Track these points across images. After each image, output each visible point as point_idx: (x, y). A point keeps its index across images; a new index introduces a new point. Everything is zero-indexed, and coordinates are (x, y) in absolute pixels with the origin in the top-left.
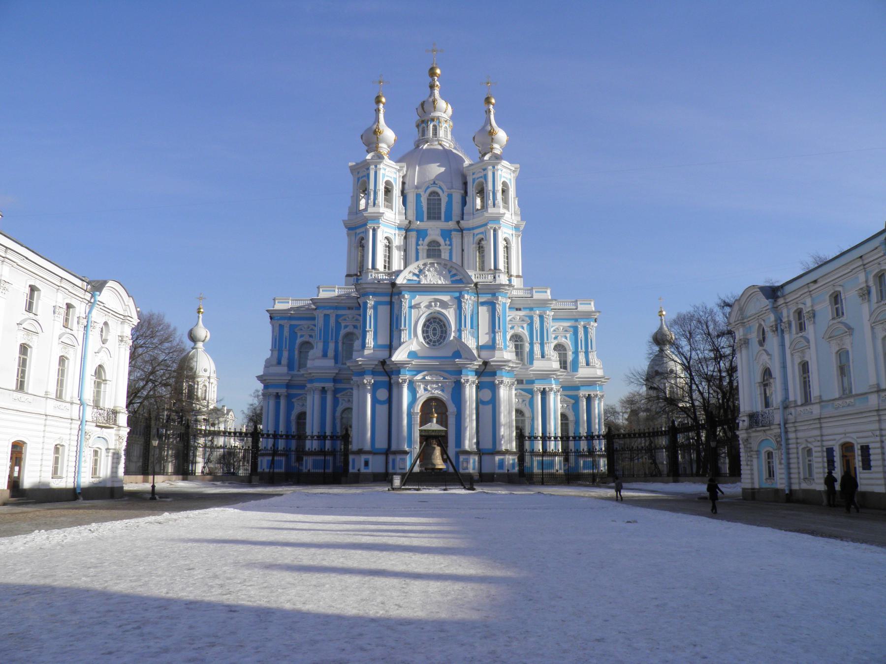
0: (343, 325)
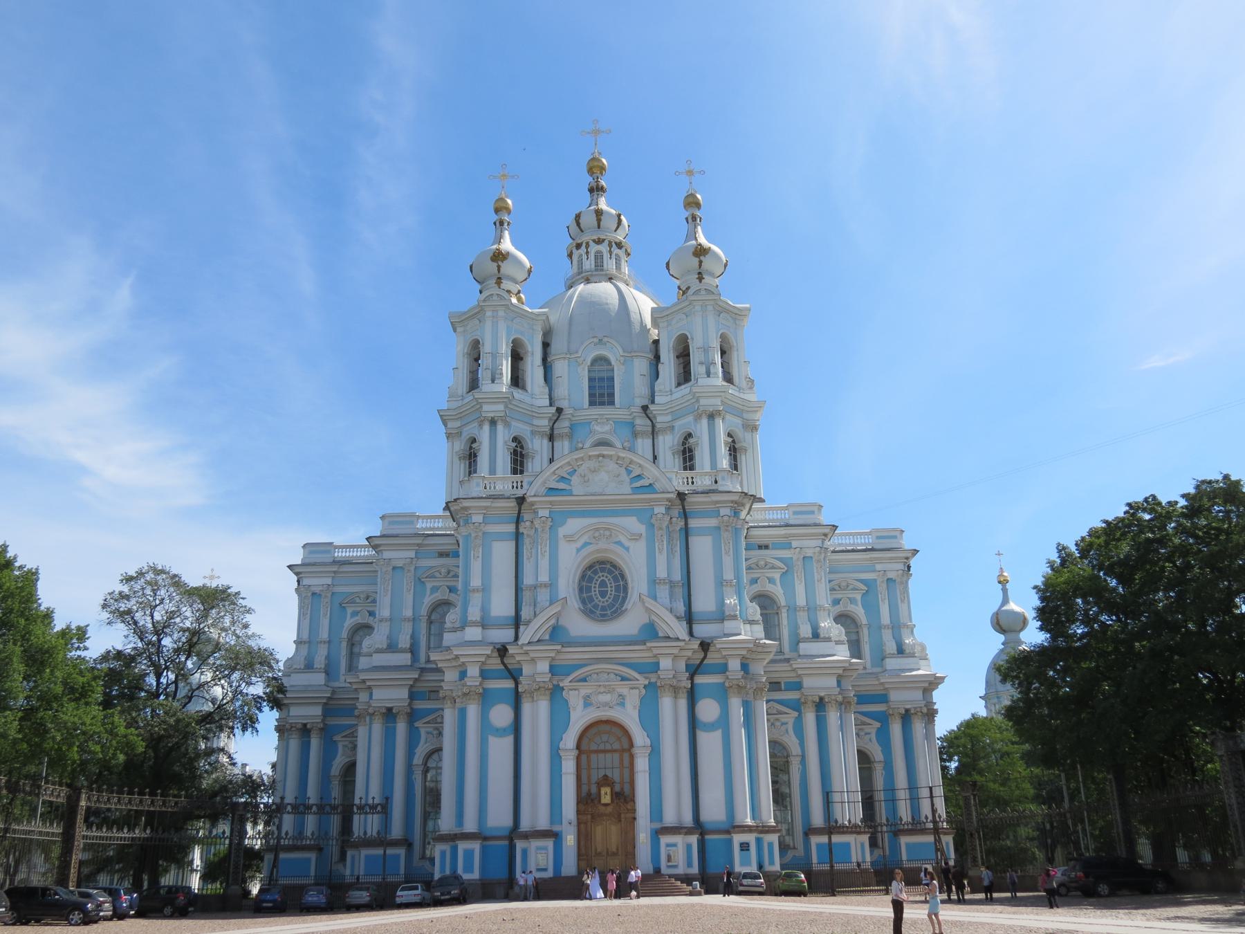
0: (429, 585)
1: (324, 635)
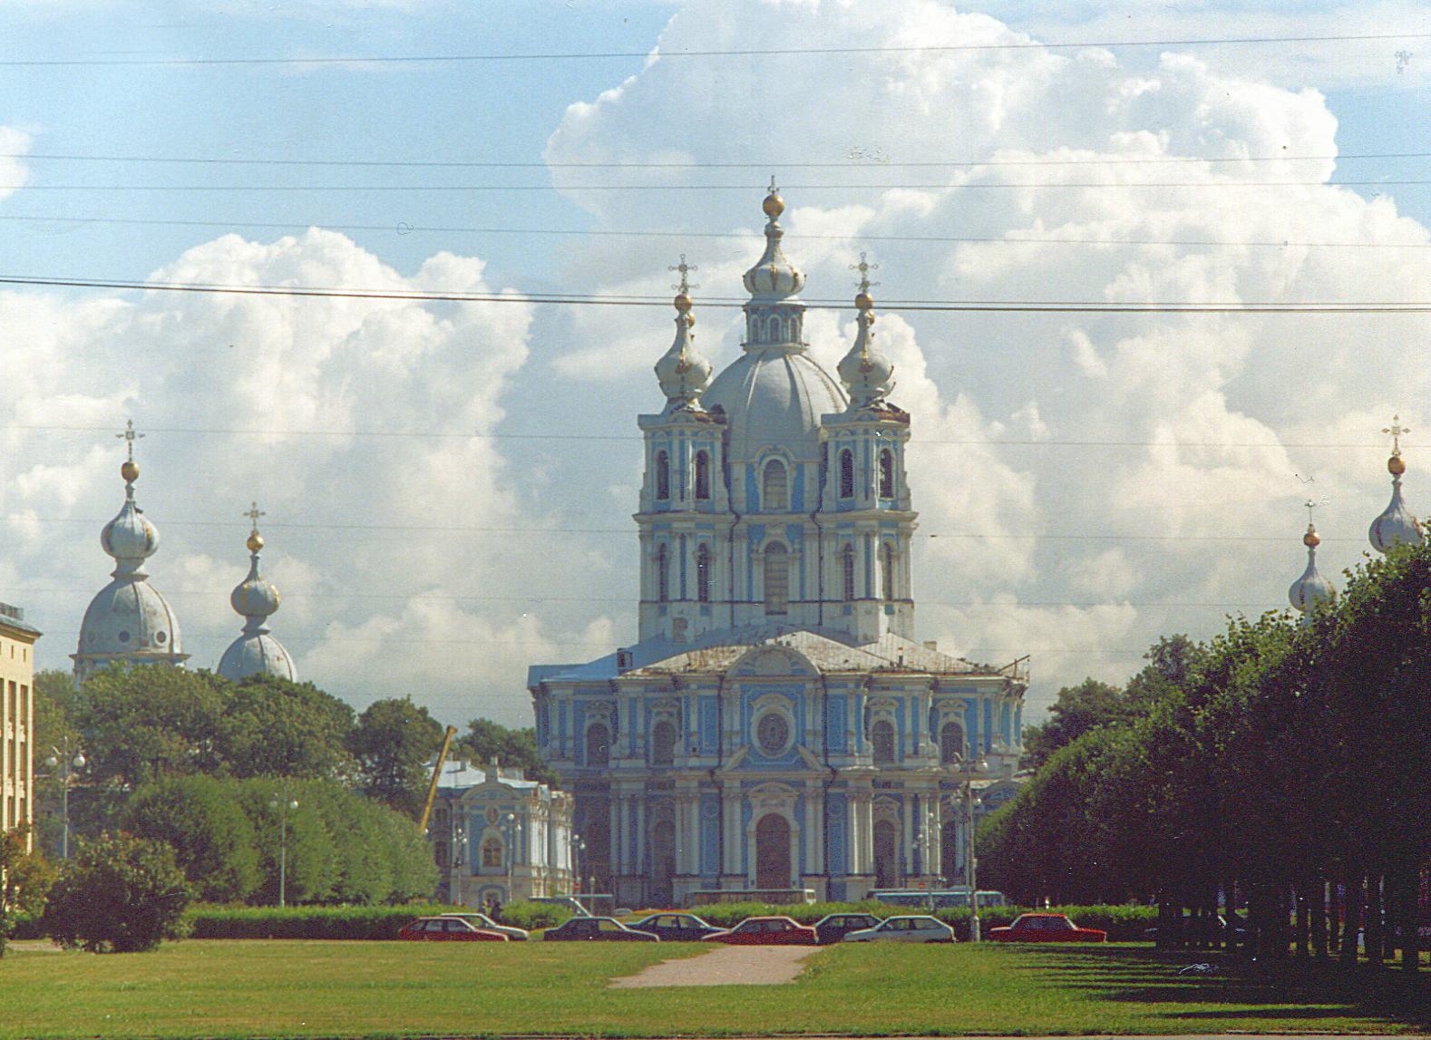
0: (655, 711)
1: (570, 732)
